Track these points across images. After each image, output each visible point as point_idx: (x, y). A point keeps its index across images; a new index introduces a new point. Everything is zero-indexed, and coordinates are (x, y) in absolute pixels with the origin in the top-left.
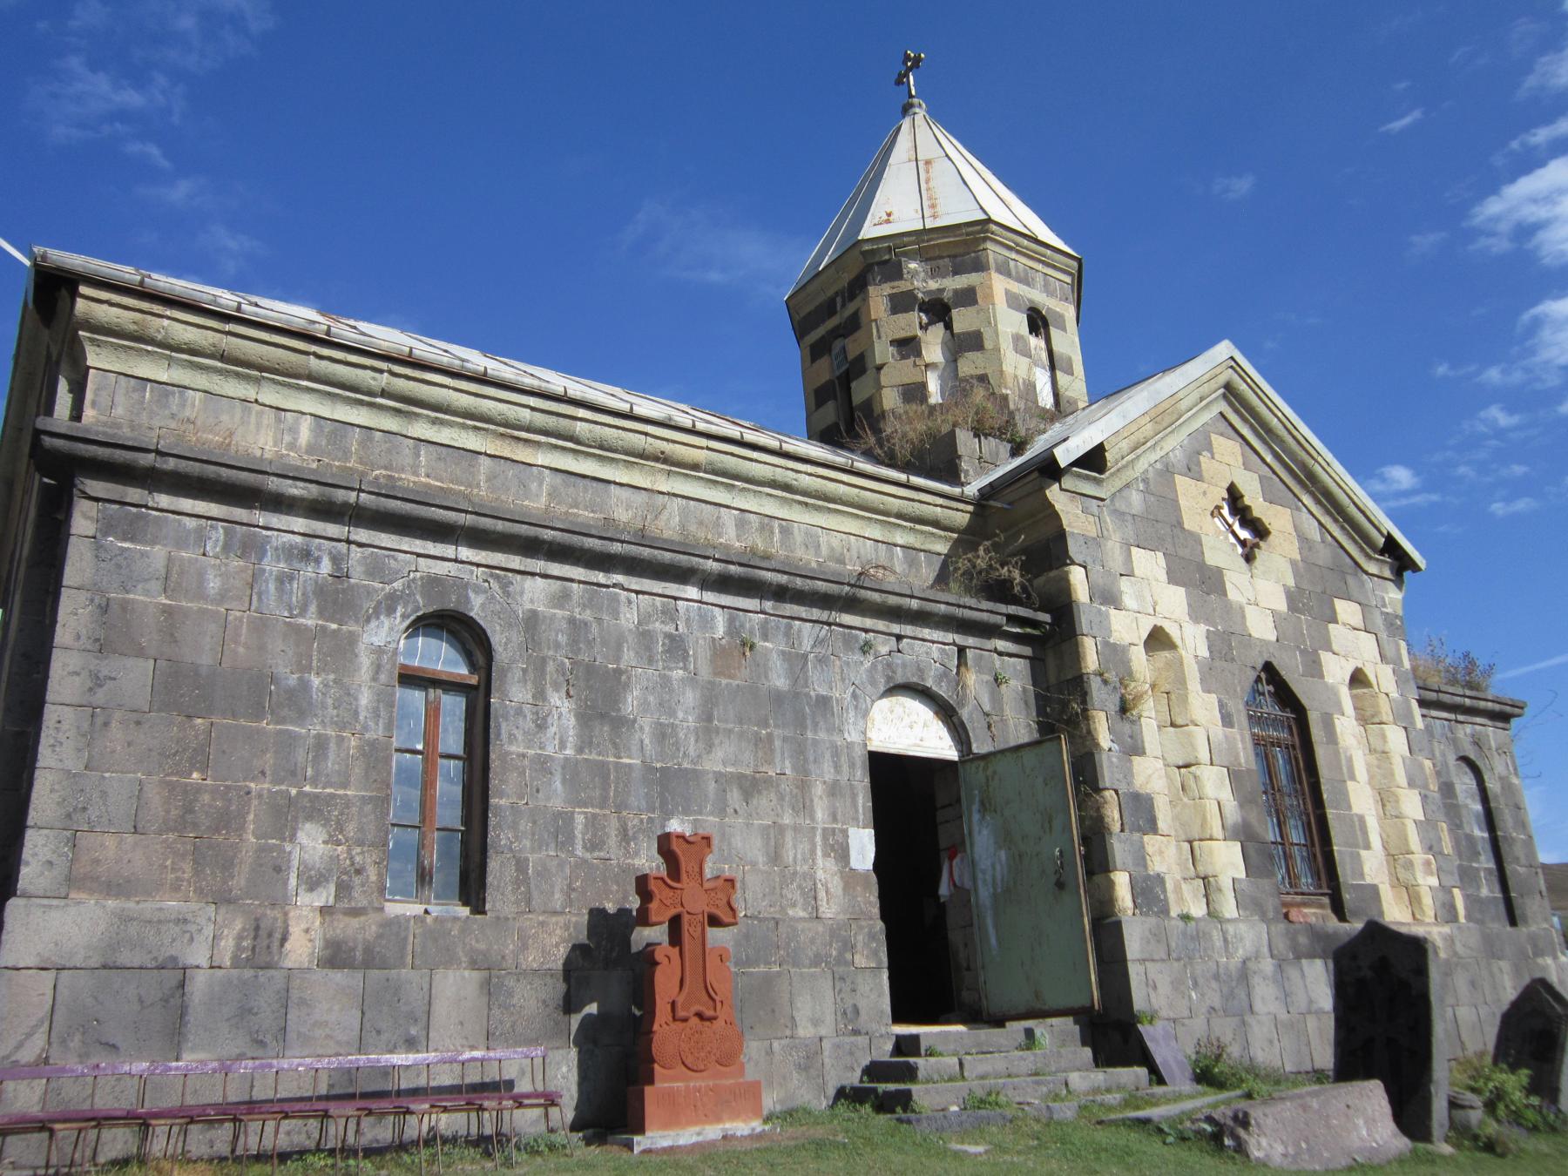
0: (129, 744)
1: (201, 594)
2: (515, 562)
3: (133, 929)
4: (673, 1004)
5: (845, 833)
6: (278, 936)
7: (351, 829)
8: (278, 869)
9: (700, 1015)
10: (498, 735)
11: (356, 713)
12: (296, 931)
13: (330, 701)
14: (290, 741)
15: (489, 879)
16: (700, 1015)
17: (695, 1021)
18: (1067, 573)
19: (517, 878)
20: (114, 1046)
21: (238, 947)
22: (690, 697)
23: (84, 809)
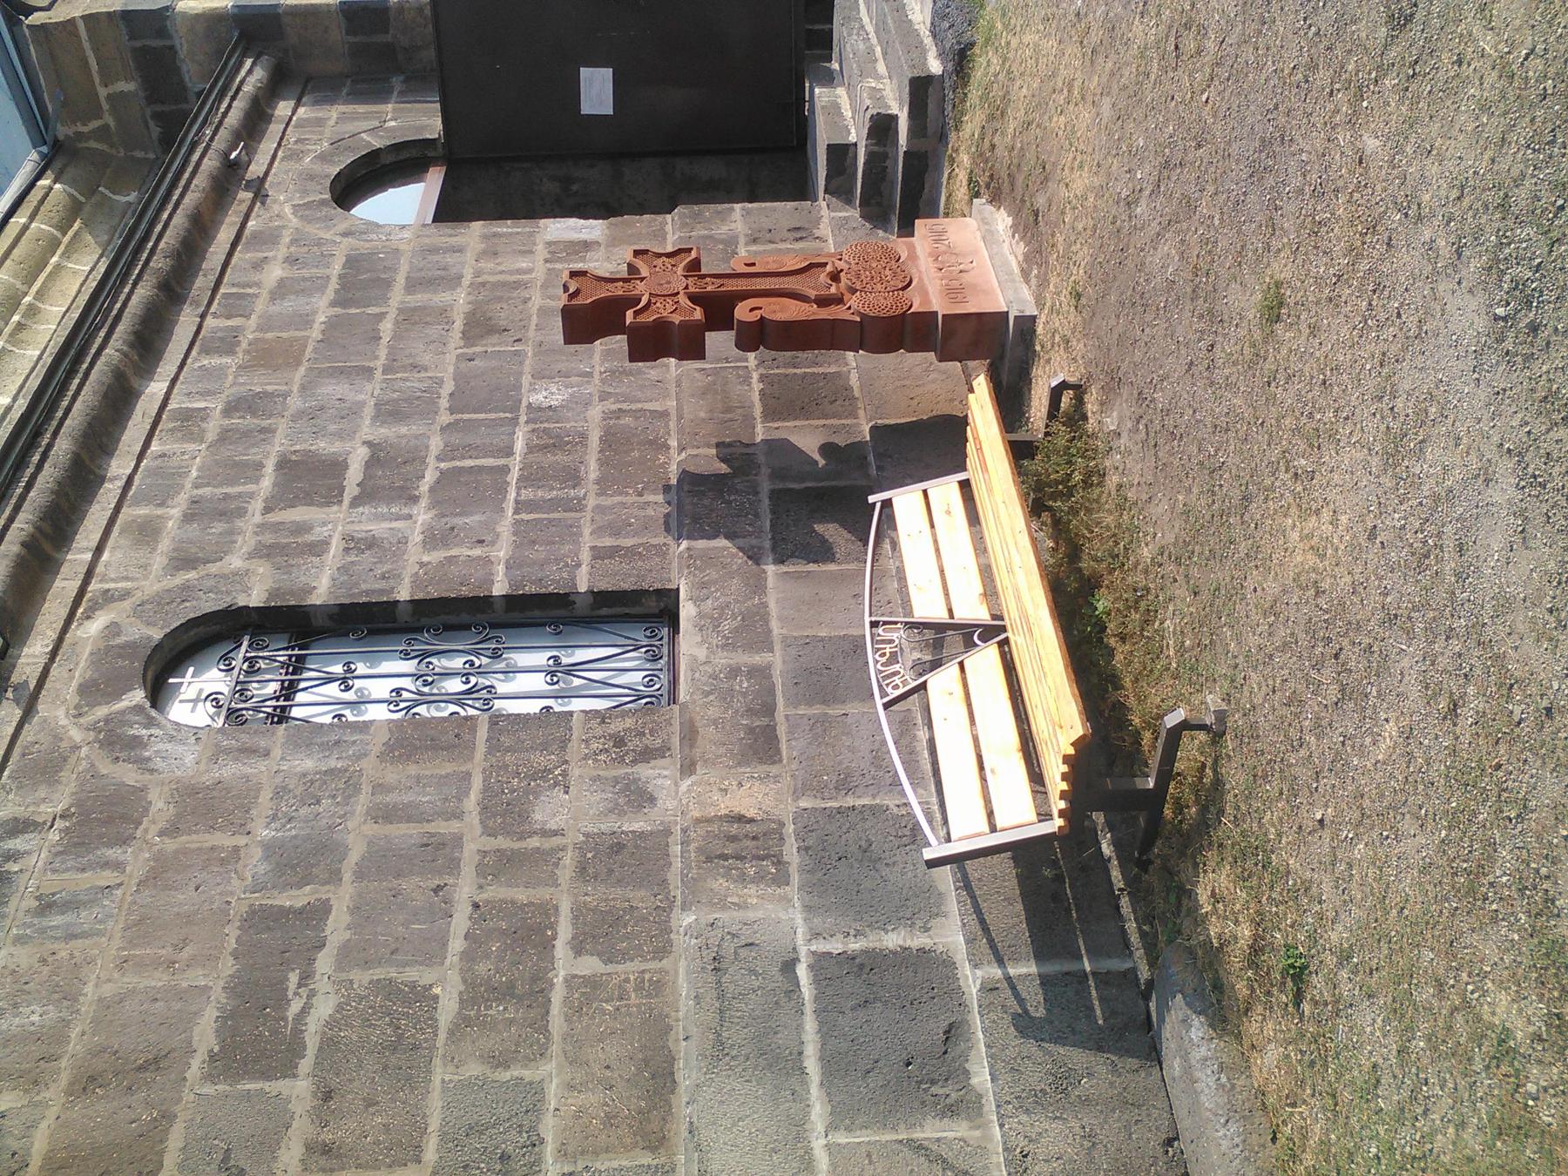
0: (370, 1103)
1: (56, 1035)
2: (64, 585)
3: (735, 1035)
5: (549, 244)
6: (735, 829)
7: (540, 760)
8: (618, 848)
10: (382, 592)
11: (330, 772)
12: (725, 805)
13: (304, 811)
14: (381, 863)
15: (626, 586)
16: (835, 277)
18: (184, 14)
20: (947, 1032)
21: (759, 878)
22: (333, 390)
23: (505, 1157)
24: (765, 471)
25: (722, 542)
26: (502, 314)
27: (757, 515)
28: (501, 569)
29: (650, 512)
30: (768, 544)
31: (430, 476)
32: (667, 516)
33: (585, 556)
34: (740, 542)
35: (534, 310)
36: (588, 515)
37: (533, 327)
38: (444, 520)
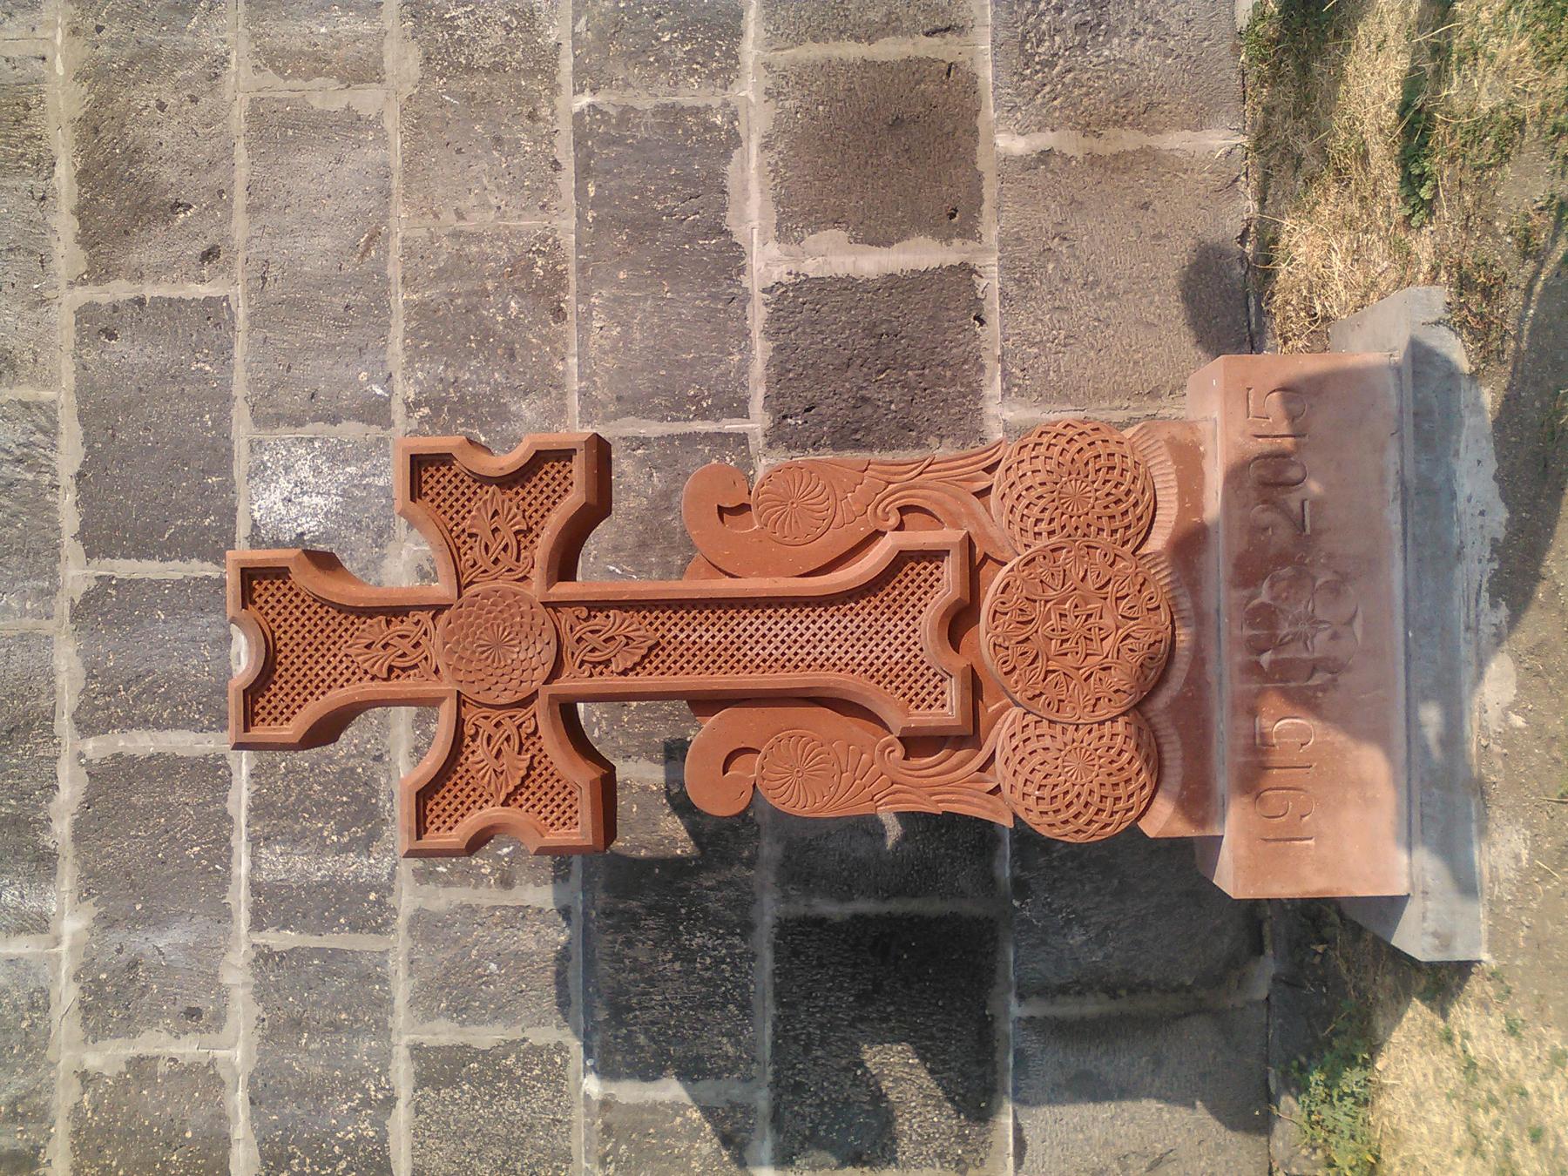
4: (918, 743)
9: (959, 621)
16: (959, 621)
17: (983, 633)
19: (478, 1080)
24: (770, 850)
25: (671, 1090)
26: (165, 138)
27: (745, 1007)
28: (238, 1100)
29: (526, 940)
30: (762, 1100)
31: (69, 791)
32: (563, 956)
33: (402, 1074)
34: (707, 1087)
35: (239, 112)
36: (397, 946)
37: (240, 199)
38: (116, 937)
